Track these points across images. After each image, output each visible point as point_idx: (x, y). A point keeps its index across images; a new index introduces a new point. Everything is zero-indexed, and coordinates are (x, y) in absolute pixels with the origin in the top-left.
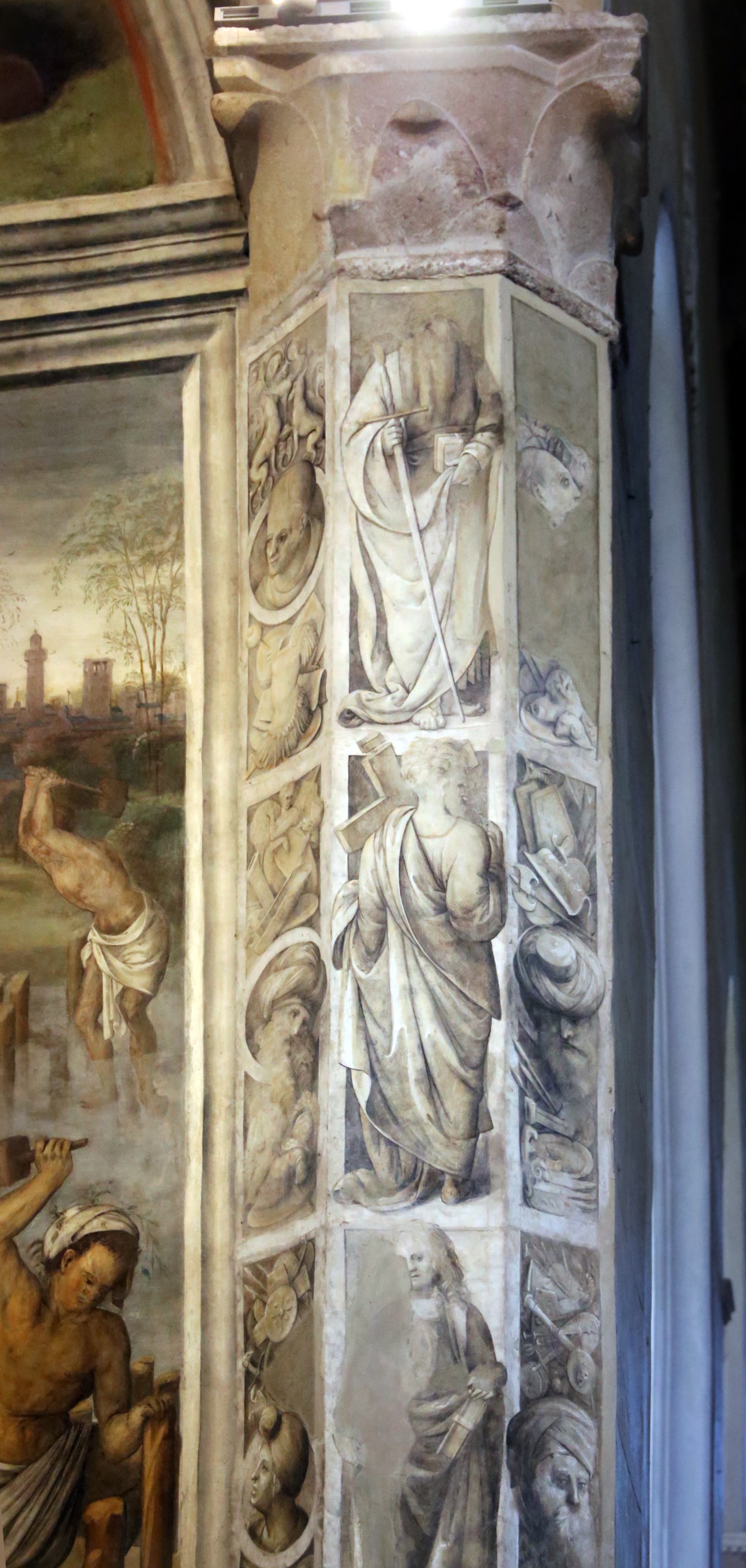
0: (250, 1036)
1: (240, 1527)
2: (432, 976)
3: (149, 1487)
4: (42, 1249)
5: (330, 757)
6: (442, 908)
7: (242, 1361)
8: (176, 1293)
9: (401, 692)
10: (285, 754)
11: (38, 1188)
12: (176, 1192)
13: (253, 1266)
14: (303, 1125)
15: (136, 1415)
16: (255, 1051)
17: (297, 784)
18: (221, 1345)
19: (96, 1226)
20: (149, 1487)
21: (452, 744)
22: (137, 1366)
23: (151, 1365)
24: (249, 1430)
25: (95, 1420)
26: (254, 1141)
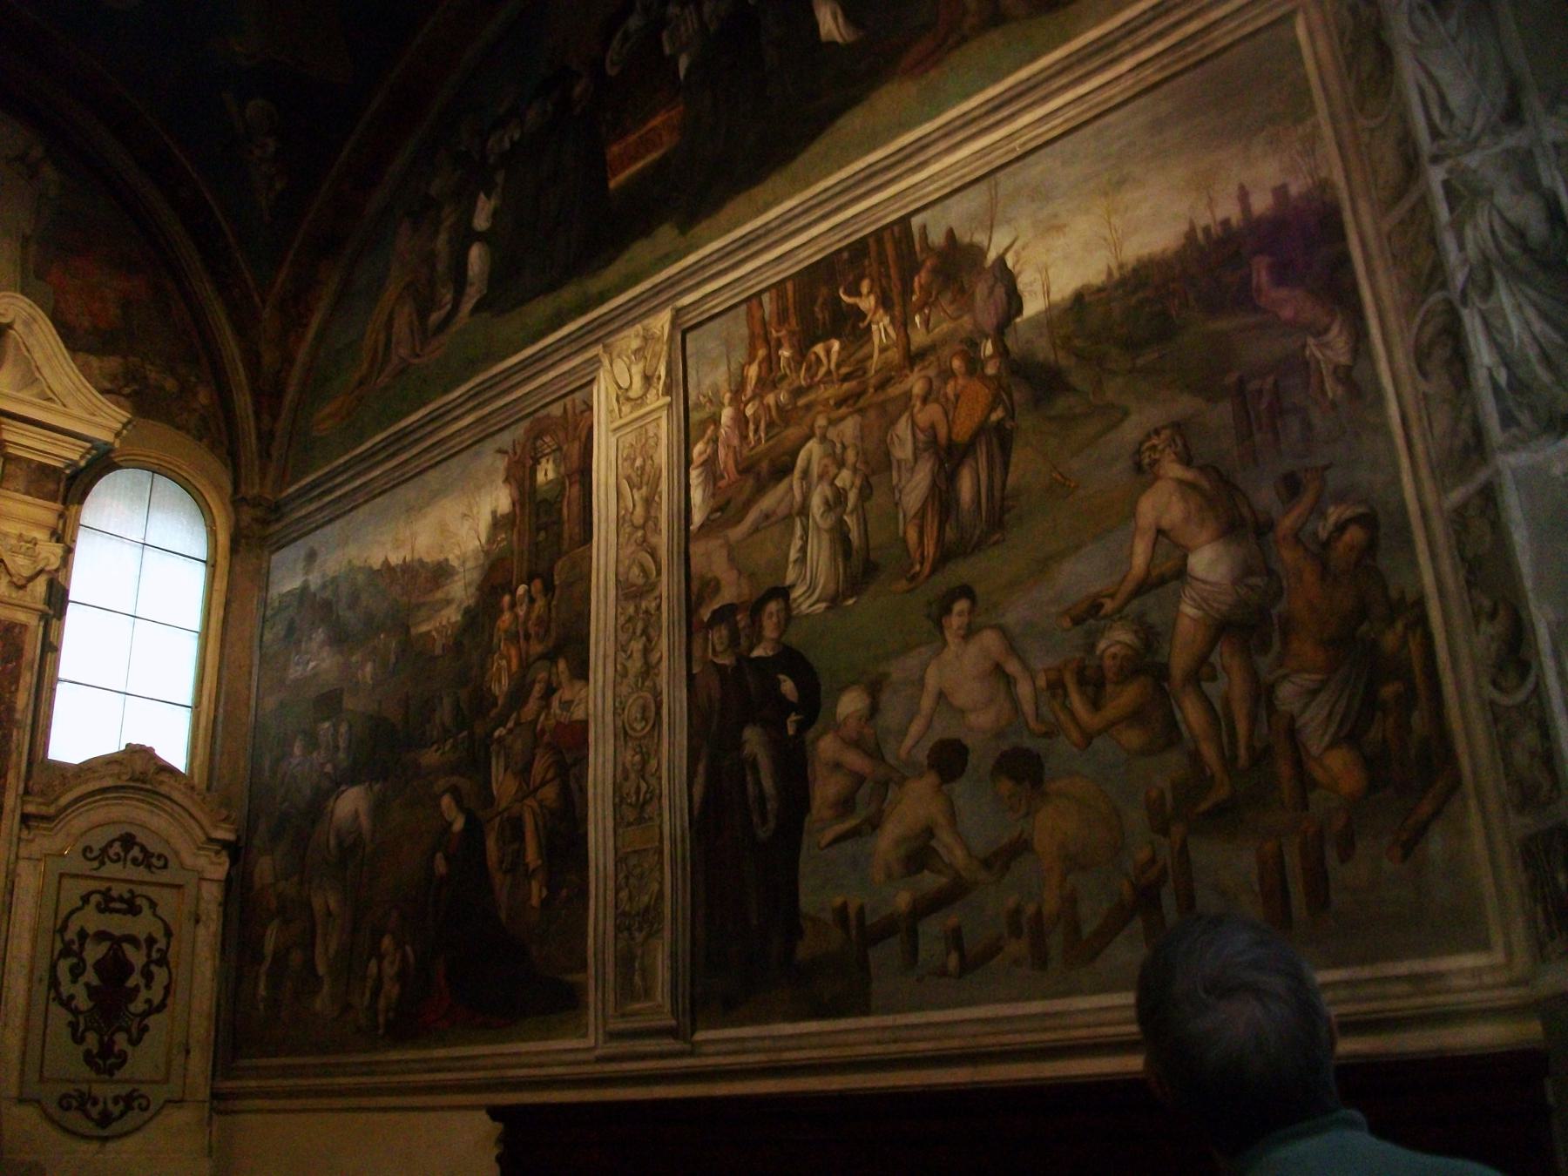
0: (1420, 367)
1: (1485, 681)
2: (1532, 294)
3: (1417, 668)
4: (1317, 537)
5: (1429, 188)
6: (1527, 249)
7: (1462, 573)
8: (1409, 543)
9: (1465, 132)
10: (1400, 193)
11: (1307, 499)
12: (1396, 480)
13: (1455, 511)
14: (1467, 412)
15: (1399, 626)
16: (1425, 375)
17: (1413, 210)
18: (1446, 566)
19: (1348, 513)
20: (1417, 668)
21: (1508, 152)
22: (1394, 594)
23: (1403, 592)
24: (1476, 616)
25: (1373, 636)
26: (1438, 430)
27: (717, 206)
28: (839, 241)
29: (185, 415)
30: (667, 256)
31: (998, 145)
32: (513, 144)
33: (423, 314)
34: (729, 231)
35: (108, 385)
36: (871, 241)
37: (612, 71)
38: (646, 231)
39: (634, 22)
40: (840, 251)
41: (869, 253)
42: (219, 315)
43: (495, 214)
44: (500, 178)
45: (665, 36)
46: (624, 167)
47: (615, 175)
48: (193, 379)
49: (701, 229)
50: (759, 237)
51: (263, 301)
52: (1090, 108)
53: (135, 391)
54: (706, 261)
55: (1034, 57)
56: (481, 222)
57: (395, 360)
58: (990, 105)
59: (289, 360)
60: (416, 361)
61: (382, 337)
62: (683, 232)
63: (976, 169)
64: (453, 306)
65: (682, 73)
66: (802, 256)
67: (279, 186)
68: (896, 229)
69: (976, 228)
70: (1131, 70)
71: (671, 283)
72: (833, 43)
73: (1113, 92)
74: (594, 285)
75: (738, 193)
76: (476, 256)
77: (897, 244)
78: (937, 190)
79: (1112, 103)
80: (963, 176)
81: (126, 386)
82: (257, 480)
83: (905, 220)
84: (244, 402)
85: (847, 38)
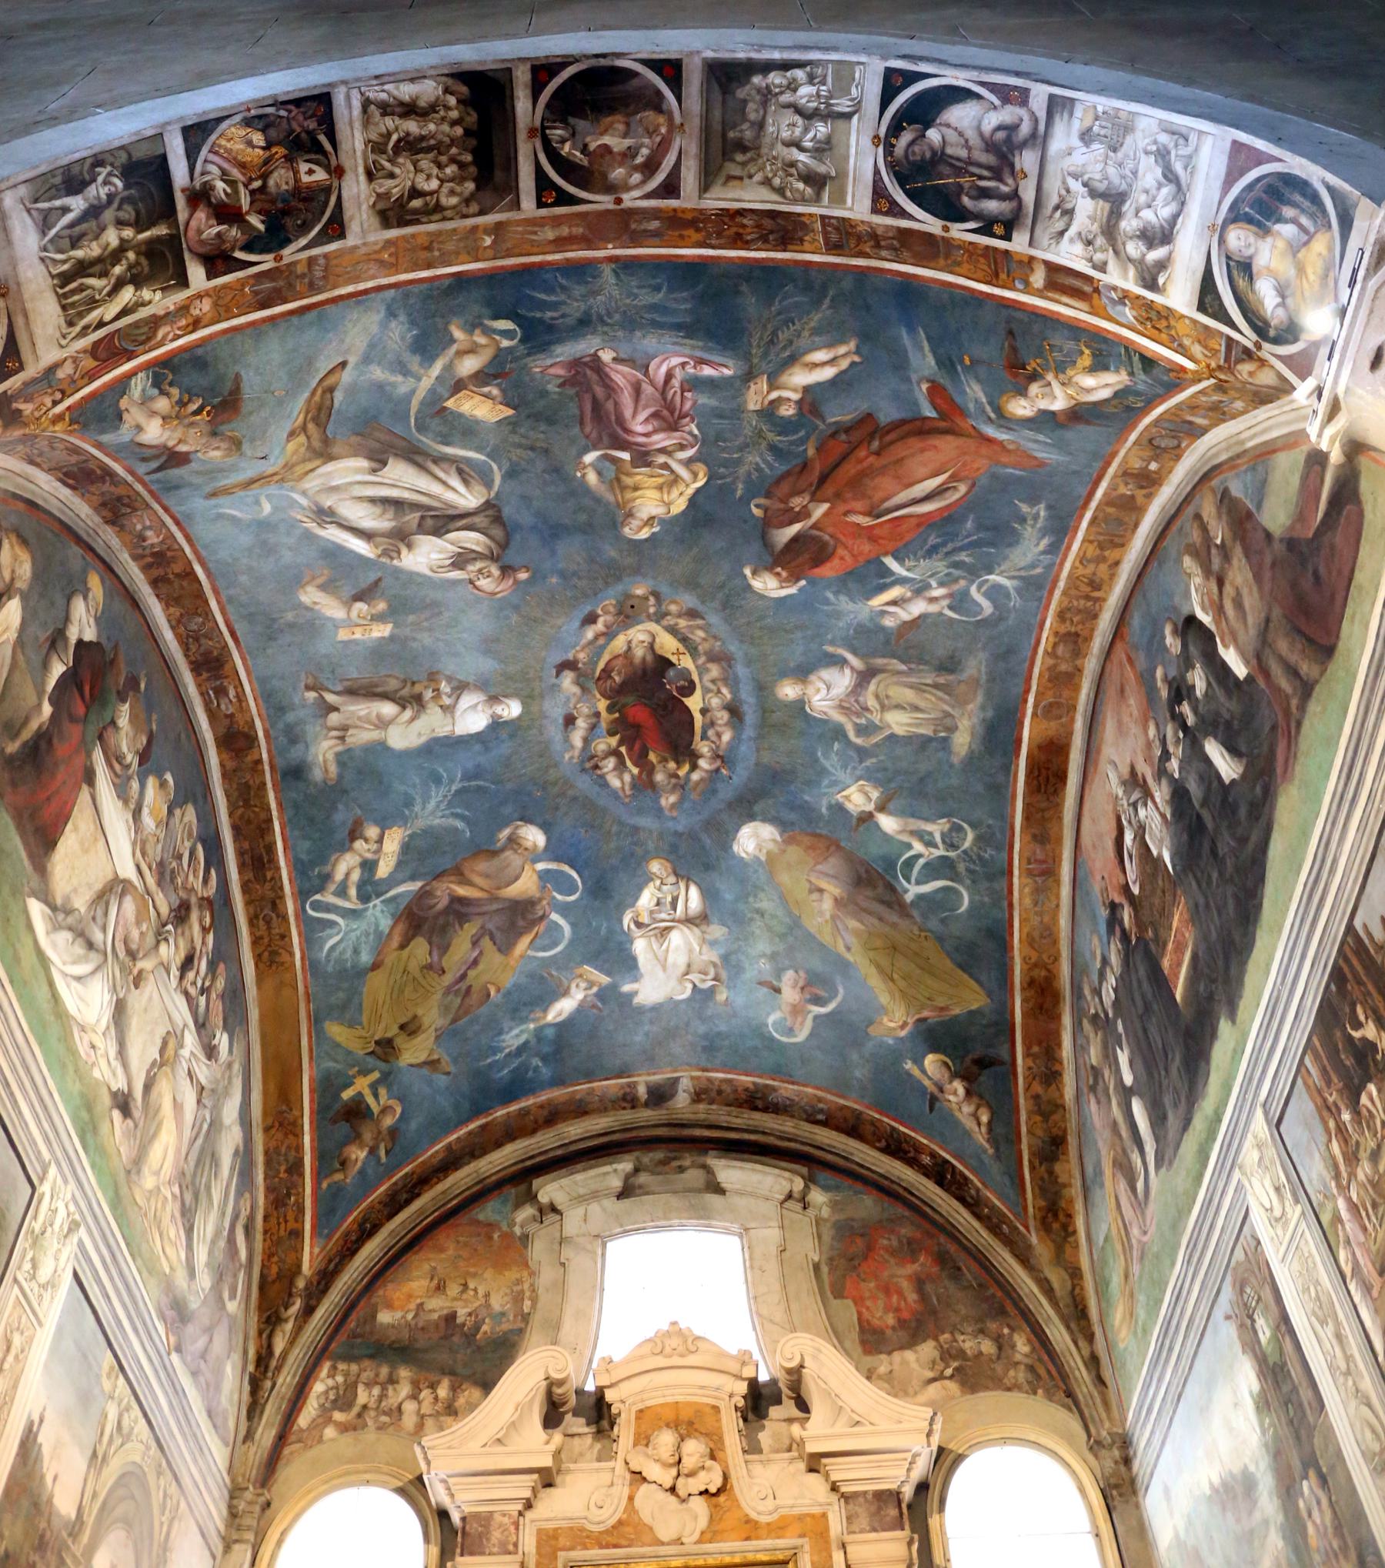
29: (1012, 1373)
32: (1115, 990)
35: (930, 1374)
39: (1129, 837)
42: (1005, 1260)
44: (1120, 1028)
48: (1006, 1331)
51: (1027, 1228)
53: (956, 1369)
59: (1075, 1274)
81: (947, 1366)
82: (1104, 1415)
84: (1059, 1334)
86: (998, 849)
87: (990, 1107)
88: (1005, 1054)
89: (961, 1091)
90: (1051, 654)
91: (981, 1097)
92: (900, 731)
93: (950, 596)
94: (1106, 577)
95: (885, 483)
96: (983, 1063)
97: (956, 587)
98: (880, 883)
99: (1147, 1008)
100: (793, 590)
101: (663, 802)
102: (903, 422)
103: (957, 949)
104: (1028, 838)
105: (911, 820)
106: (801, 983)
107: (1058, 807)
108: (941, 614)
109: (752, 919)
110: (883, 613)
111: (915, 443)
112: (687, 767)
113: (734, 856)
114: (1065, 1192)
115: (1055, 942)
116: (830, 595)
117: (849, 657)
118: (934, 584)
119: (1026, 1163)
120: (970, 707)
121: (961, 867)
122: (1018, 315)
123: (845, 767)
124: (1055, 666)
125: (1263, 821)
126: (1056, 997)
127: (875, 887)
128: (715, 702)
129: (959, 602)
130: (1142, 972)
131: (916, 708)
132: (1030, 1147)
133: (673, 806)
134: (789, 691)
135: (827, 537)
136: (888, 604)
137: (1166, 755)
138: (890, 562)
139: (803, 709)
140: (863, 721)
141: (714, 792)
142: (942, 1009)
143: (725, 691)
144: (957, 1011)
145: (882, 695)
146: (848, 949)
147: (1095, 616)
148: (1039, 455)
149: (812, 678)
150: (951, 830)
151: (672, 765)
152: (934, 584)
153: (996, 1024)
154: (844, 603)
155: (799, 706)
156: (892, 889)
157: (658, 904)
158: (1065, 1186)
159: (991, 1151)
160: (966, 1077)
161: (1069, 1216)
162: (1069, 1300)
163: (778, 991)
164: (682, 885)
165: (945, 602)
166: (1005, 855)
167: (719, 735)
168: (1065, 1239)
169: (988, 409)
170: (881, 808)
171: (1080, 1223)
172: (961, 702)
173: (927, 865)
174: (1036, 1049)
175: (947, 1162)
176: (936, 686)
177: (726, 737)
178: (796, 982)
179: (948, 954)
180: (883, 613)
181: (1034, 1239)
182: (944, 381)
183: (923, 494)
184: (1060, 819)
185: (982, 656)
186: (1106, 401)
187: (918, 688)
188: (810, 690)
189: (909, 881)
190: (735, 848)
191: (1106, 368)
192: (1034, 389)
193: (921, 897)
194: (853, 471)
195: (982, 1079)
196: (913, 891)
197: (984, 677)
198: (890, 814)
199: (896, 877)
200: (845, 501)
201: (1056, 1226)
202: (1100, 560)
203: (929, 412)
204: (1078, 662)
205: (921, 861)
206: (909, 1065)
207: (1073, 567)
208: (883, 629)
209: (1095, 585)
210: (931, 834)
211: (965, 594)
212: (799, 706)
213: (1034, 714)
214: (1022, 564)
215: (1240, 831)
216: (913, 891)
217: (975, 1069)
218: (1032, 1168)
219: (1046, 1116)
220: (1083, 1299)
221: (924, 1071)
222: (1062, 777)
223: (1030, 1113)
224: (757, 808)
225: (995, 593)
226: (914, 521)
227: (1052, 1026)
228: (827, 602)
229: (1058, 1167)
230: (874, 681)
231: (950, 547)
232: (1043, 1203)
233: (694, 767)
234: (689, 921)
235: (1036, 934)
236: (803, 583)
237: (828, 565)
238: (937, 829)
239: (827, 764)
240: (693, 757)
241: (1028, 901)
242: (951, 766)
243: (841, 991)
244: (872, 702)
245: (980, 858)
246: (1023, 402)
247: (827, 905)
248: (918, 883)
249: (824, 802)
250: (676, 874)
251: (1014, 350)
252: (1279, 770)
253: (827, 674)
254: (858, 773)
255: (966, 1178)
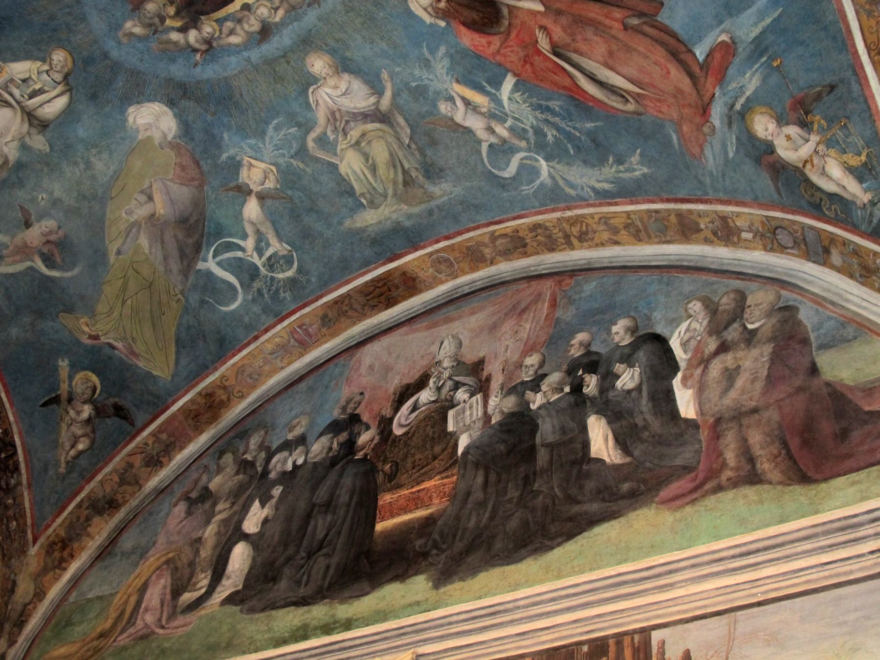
27: (474, 571)
28: (582, 634)
30: (418, 603)
31: (742, 587)
32: (295, 466)
33: (176, 593)
34: (480, 598)
36: (611, 642)
37: (398, 431)
38: (401, 577)
39: (425, 396)
40: (580, 643)
41: (608, 652)
43: (266, 521)
44: (277, 491)
45: (451, 413)
46: (392, 516)
47: (383, 519)
49: (454, 588)
50: (506, 611)
51: (34, 542)
52: (831, 576)
54: (455, 618)
55: (782, 520)
56: (251, 525)
57: (139, 623)
58: (737, 551)
59: (40, 595)
60: (158, 631)
61: (133, 600)
62: (436, 586)
63: (720, 603)
64: (206, 593)
65: (460, 451)
66: (544, 638)
67: (81, 447)
68: (637, 638)
69: (712, 657)
70: (872, 552)
71: (415, 628)
72: (600, 461)
73: (853, 567)
74: (344, 611)
75: (494, 566)
76: (240, 555)
77: (636, 651)
78: (679, 612)
79: (852, 577)
80: (705, 606)
83: (645, 632)
85: (614, 459)
86: (294, 299)
87: (91, 447)
88: (140, 420)
89: (85, 415)
90: (493, 237)
91: (93, 431)
92: (343, 169)
93: (504, 141)
94: (597, 241)
95: (600, 48)
96: (120, 411)
97: (515, 141)
98: (196, 237)
99: (328, 505)
100: (428, 19)
101: (128, 25)
102: (674, 35)
103: (189, 327)
104: (321, 314)
105: (268, 224)
106: (53, 238)
107: (363, 316)
108: (479, 142)
109: (76, 164)
110: (451, 99)
111: (660, 54)
112: (178, 24)
113: (123, 111)
114: (84, 538)
115: (254, 387)
116: (442, 50)
117: (388, 94)
118: (509, 123)
119: (78, 499)
120: (404, 207)
121: (256, 285)
122: (855, 87)
123: (277, 148)
124: (485, 245)
125: (614, 507)
126: (214, 418)
127: (189, 236)
128: (263, 12)
129: (502, 150)
130: (348, 481)
131: (374, 169)
132: (92, 491)
133: (131, 35)
134: (318, 64)
135: (506, 23)
136: (463, 99)
137: (535, 385)
138: (509, 83)
139: (309, 85)
140: (332, 137)
141: (173, 60)
142: (133, 353)
143: (281, 13)
144: (141, 364)
145: (368, 137)
146: (119, 252)
147: (552, 250)
148: (708, 152)
149: (346, 76)
150: (284, 256)
151: (171, 10)
152: (509, 123)
153: (158, 397)
154: (441, 66)
155: (311, 81)
156: (198, 248)
157: (24, 81)
158: (89, 535)
159: (62, 470)
160: (99, 411)
161: (72, 556)
162: (19, 608)
163: (28, 225)
164: (60, 89)
165: (493, 140)
166: (293, 307)
167: (232, 32)
168: (55, 568)
169: (742, 100)
170: (262, 197)
171: (74, 567)
172: (400, 198)
173: (240, 259)
174: (164, 436)
175: (14, 446)
176: (405, 172)
177: (234, 40)
178: (51, 233)
179: (179, 325)
180: (451, 99)
181: (33, 550)
182: (742, 52)
183: (604, 79)
184: (354, 324)
185: (458, 190)
186: (819, 189)
187: (394, 161)
188: (331, 82)
189: (214, 257)
190: (131, 109)
191: (860, 179)
192: (793, 130)
193: (209, 274)
194: (592, 15)
195: (107, 420)
196: (210, 264)
197: (438, 202)
198: (262, 206)
199: (209, 245)
200: (555, 21)
201: (57, 554)
202: (615, 231)
203: (700, 53)
204: (498, 258)
205: (239, 254)
206: (64, 364)
207: (592, 216)
208: (435, 106)
209: (583, 237)
210: (268, 245)
211: (513, 150)
212: (311, 81)
213: (430, 254)
214: (571, 179)
215: (574, 491)
216: (210, 264)
217: (111, 411)
218: (79, 506)
219: (123, 482)
220: (30, 615)
221: (71, 378)
222: (390, 303)
223: (115, 470)
224: (184, 103)
225: (528, 171)
226: (567, 82)
227: (190, 432)
228: (433, 51)
229: (96, 520)
230: (377, 125)
231: (557, 120)
232: (63, 534)
233: (183, 30)
234: (30, 116)
235: (249, 370)
236: (443, 24)
237: (476, 36)
238: (276, 246)
239: (270, 130)
240: (193, 23)
241: (269, 347)
242: (340, 223)
243: (76, 271)
244: (354, 134)
245: (277, 290)
246: (772, 126)
247: (142, 212)
248: (219, 264)
249: (232, 152)
250: (66, 77)
251: (819, 97)
252: (665, 493)
253: (358, 86)
254: (281, 161)
255: (17, 468)
